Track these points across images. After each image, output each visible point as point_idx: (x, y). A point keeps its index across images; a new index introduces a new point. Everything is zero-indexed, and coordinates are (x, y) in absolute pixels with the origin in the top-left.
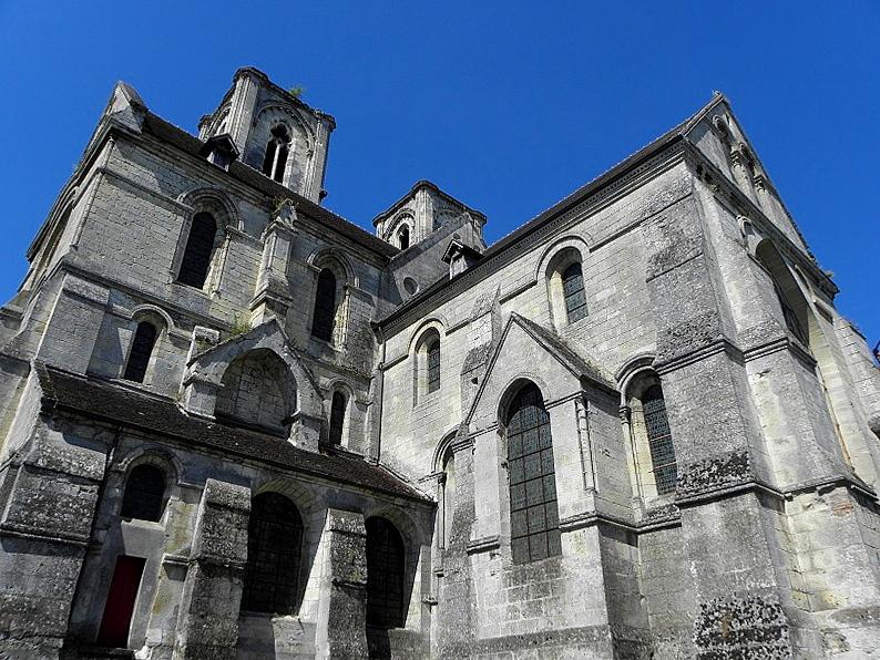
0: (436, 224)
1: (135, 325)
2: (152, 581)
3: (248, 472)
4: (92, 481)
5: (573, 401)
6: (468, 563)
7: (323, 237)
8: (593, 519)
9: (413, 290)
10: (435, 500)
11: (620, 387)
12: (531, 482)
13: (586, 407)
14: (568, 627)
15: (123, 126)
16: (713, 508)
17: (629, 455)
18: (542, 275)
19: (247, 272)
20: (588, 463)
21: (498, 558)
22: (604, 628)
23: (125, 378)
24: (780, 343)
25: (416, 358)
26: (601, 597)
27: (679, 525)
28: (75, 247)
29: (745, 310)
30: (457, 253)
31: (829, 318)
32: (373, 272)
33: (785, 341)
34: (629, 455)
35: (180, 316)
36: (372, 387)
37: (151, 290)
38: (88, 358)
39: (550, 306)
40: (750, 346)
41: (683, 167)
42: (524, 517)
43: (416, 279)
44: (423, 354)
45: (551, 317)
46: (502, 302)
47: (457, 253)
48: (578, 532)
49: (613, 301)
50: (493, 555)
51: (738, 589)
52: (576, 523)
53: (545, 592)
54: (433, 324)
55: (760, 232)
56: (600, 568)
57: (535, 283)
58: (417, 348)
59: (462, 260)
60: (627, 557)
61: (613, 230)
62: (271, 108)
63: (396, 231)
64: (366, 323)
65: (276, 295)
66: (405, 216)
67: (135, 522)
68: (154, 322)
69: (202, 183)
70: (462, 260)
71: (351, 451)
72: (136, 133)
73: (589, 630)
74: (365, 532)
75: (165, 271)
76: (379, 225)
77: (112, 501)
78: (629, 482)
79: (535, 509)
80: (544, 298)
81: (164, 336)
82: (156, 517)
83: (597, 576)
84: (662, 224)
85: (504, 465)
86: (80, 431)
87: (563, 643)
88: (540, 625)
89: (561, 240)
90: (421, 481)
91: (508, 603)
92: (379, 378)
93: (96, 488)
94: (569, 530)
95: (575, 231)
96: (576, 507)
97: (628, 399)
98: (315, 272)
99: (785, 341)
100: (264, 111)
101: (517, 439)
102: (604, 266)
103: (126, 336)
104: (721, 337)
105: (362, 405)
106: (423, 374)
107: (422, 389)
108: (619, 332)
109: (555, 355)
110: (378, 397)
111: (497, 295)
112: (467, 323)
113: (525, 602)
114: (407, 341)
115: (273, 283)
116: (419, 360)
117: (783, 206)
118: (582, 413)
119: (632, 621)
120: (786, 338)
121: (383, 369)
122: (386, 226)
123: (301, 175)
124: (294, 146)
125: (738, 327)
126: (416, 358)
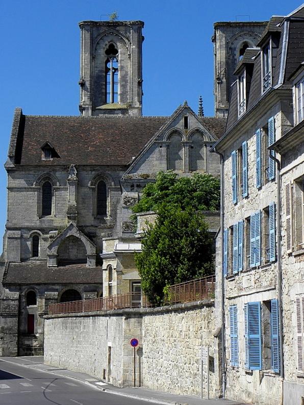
1: (31, 239)
3: (57, 287)
4: (16, 300)
7: (94, 170)
15: (9, 167)
23: (33, 256)
28: (8, 220)
35: (42, 230)
37: (33, 225)
38: (19, 256)
62: (101, 39)
65: (70, 214)
67: (30, 306)
69: (41, 173)
72: (13, 168)
75: (36, 216)
86: (12, 287)
98: (93, 189)
100: (98, 43)
103: (29, 243)
115: (70, 208)
123: (127, 74)
124: (120, 55)
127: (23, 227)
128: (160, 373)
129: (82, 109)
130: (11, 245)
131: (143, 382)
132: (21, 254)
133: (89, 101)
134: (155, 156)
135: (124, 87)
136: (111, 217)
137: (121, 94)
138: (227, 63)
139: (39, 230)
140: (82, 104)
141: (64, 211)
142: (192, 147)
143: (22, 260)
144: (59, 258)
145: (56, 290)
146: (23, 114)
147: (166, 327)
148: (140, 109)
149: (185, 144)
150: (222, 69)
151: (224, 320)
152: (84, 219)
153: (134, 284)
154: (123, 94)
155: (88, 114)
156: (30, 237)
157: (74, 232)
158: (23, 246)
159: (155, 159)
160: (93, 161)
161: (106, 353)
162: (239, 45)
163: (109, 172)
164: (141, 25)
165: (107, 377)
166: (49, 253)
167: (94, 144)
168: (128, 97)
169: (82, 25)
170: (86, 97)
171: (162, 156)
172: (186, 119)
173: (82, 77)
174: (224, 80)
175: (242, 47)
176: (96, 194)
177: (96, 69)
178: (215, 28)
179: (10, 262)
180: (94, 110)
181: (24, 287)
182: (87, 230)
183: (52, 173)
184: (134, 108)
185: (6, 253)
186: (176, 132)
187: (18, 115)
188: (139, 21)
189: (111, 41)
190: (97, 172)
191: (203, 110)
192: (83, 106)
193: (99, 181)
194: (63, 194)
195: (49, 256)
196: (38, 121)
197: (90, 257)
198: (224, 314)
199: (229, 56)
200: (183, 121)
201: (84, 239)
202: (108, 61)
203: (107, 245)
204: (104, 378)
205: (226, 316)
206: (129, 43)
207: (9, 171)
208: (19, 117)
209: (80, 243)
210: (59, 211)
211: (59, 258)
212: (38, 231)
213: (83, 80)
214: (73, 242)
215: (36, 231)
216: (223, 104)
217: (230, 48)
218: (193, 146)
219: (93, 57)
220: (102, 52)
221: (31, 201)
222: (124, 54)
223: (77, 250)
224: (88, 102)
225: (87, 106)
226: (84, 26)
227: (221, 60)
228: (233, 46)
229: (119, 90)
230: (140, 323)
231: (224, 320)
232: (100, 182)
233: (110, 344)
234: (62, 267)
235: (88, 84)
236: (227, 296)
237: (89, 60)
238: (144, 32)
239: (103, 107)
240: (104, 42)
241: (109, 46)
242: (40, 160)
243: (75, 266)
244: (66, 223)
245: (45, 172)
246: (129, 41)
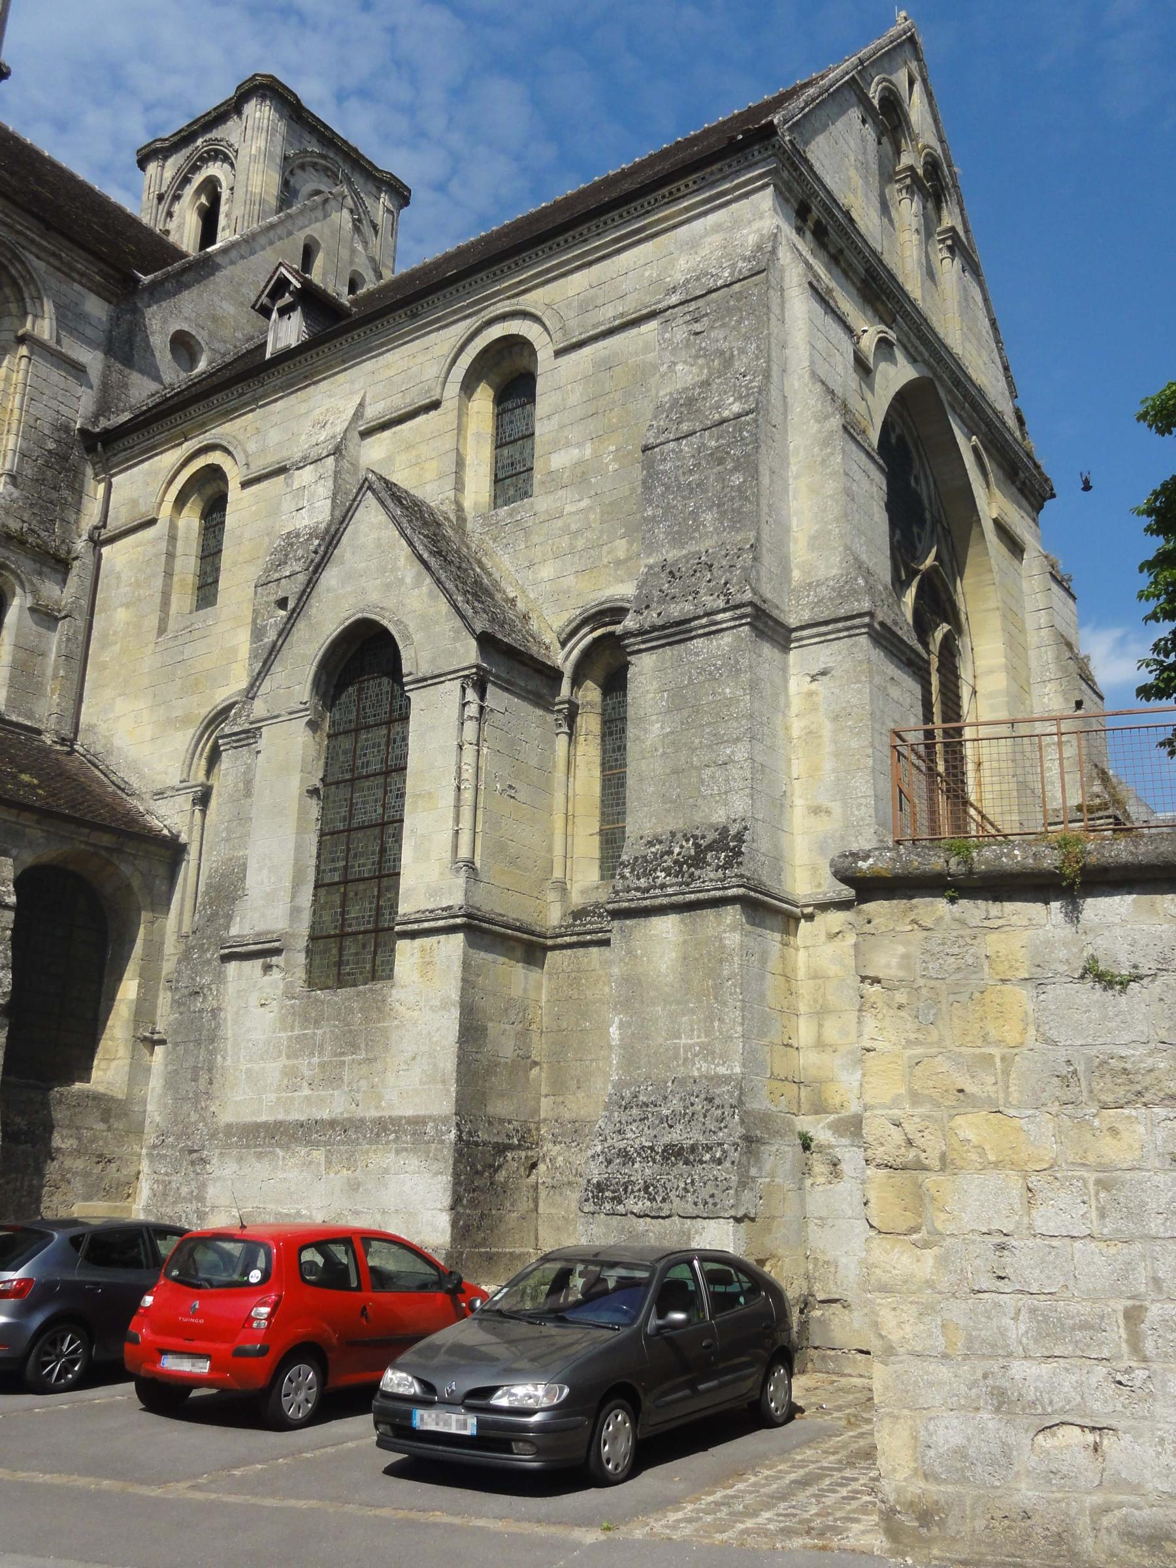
0: (288, 193)
5: (458, 683)
6: (220, 978)
8: (459, 921)
9: (193, 361)
10: (183, 838)
11: (564, 659)
12: (360, 834)
13: (482, 697)
14: (386, 1114)
16: (667, 927)
17: (559, 797)
18: (453, 389)
20: (466, 812)
21: (276, 975)
22: (445, 1120)
24: (857, 621)
25: (173, 527)
26: (449, 1064)
27: (606, 943)
29: (816, 542)
30: (287, 298)
31: (1016, 548)
32: (96, 308)
33: (867, 620)
34: (559, 797)
36: (73, 580)
39: (460, 463)
40: (806, 616)
41: (766, 199)
42: (337, 898)
43: (201, 336)
44: (191, 520)
45: (459, 486)
46: (365, 434)
47: (287, 298)
48: (432, 940)
49: (581, 476)
50: (267, 968)
51: (681, 1072)
52: (426, 925)
53: (354, 1047)
54: (215, 458)
55: (913, 360)
56: (455, 1013)
57: (435, 405)
58: (181, 501)
59: (297, 317)
60: (516, 992)
61: (608, 315)
63: (189, 190)
64: (66, 429)
66: (217, 155)
70: (297, 317)
71: (14, 718)
73: (418, 1122)
74: (12, 900)
76: (152, 167)
78: (550, 849)
79: (361, 886)
80: (449, 442)
83: (449, 1025)
84: (697, 327)
85: (314, 792)
87: (370, 1142)
88: (335, 1105)
89: (503, 317)
90: (160, 794)
91: (283, 1061)
92: (89, 560)
94: (413, 935)
95: (533, 300)
96: (433, 893)
97: (576, 682)
99: (867, 620)
101: (346, 743)
102: (575, 396)
104: (748, 596)
105: (46, 616)
106: (188, 564)
107: (183, 598)
108: (580, 543)
109: (438, 582)
110: (84, 603)
111: (358, 414)
112: (282, 470)
113: (316, 1060)
114: (158, 486)
116: (181, 533)
117: (986, 300)
118: (472, 710)
119: (498, 1107)
120: (870, 614)
121: (97, 542)
122: (169, 174)
125: (796, 574)
126: (173, 527)
136: (15, 485)
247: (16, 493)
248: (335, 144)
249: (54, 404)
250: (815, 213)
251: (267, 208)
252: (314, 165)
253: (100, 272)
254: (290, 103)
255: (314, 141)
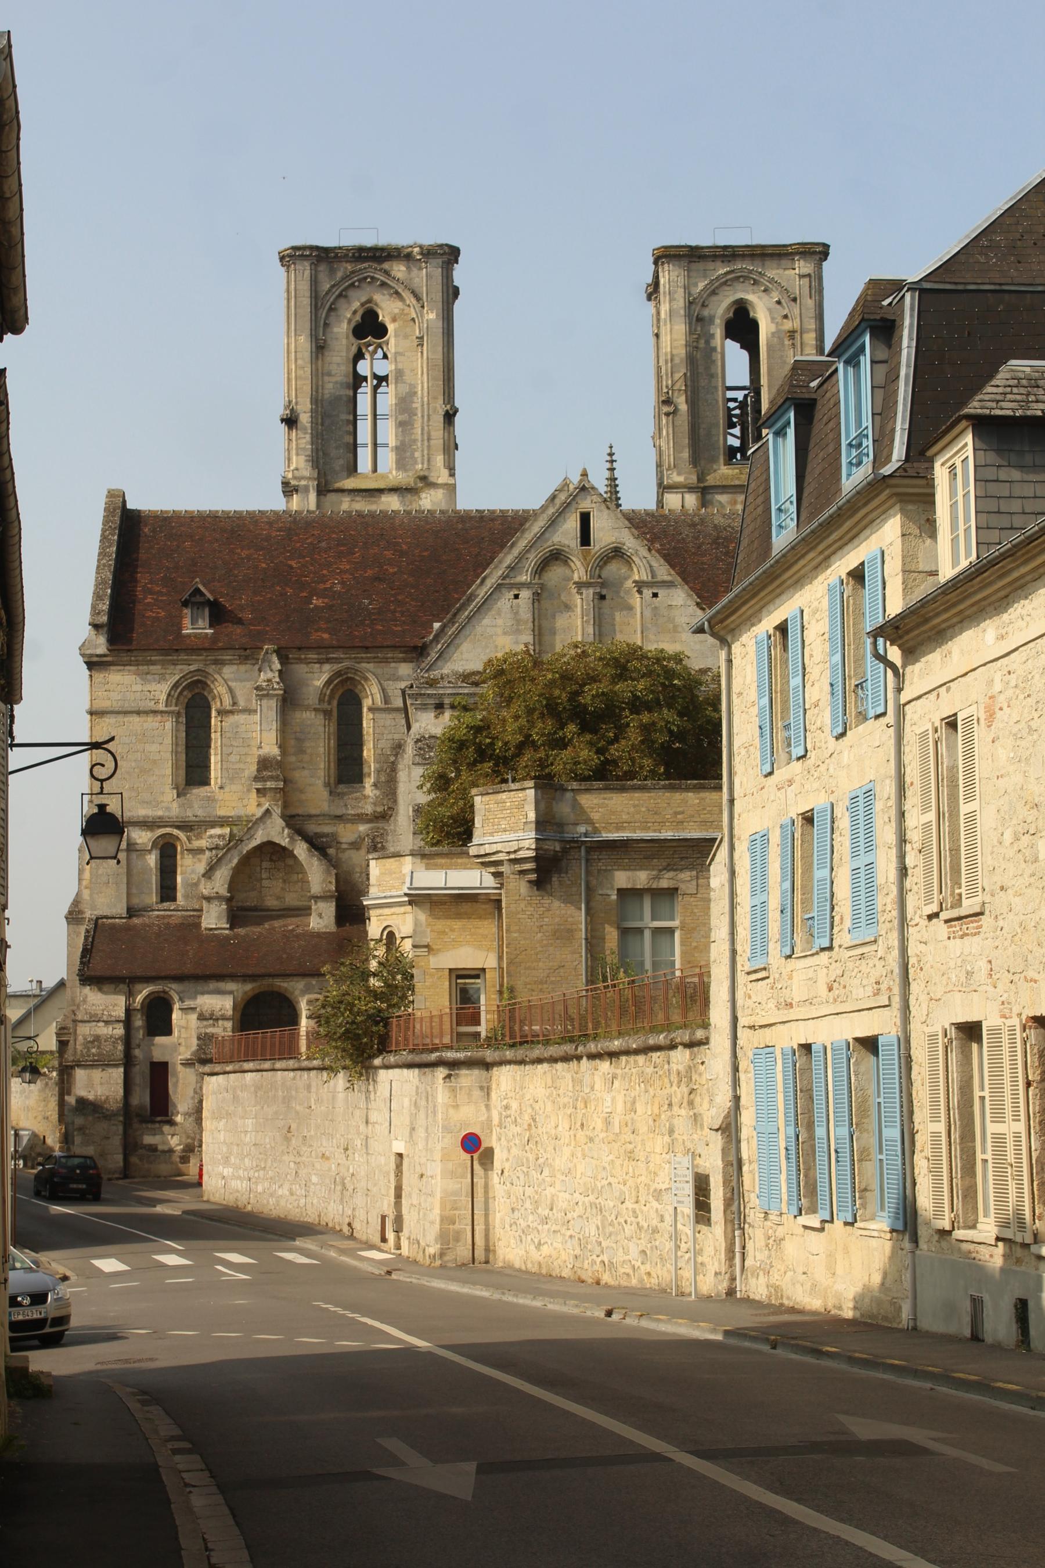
2: (175, 1074)
3: (231, 986)
7: (328, 661)
15: (91, 656)
19: (244, 751)
37: (160, 813)
38: (125, 900)
62: (340, 295)
68: (171, 841)
72: (105, 656)
77: (138, 1029)
81: (182, 853)
82: (168, 1031)
86: (106, 988)
93: (121, 1025)
100: (331, 309)
115: (264, 763)
124: (392, 342)
127: (135, 820)
128: (546, 1227)
129: (289, 489)
130: (100, 872)
131: (494, 1251)
132: (129, 895)
133: (309, 469)
134: (500, 622)
135: (404, 426)
137: (397, 448)
138: (691, 360)
139: (178, 827)
140: (290, 476)
141: (247, 773)
142: (603, 597)
143: (132, 912)
144: (234, 904)
145: (231, 992)
146: (129, 506)
147: (566, 1100)
148: (451, 489)
149: (580, 585)
150: (677, 376)
151: (736, 1083)
152: (303, 797)
153: (459, 981)
154: (403, 452)
155: (306, 503)
156: (155, 844)
157: (276, 831)
158: (135, 871)
159: (499, 631)
160: (326, 636)
161: (388, 1173)
162: (721, 309)
163: (371, 665)
164: (450, 255)
165: (391, 1236)
166: (205, 892)
167: (326, 589)
168: (417, 454)
169: (289, 256)
170: (302, 458)
171: (518, 622)
172: (585, 519)
173: (290, 402)
174: (683, 407)
175: (731, 315)
176: (333, 728)
177: (326, 378)
178: (656, 263)
179: (97, 919)
180: (323, 490)
181: (138, 986)
182: (312, 828)
183: (211, 669)
184: (433, 485)
185: (86, 894)
186: (557, 557)
187: (114, 510)
188: (447, 245)
189: (370, 301)
190: (336, 667)
191: (617, 486)
192: (293, 482)
193: (340, 692)
194: (243, 728)
195: (208, 899)
196: (166, 521)
197: (316, 898)
198: (736, 1069)
199: (697, 340)
200: (572, 524)
201: (301, 850)
202: (359, 356)
203: (381, 874)
204: (384, 1240)
205: (742, 1076)
206: (418, 306)
207: (93, 664)
208: (117, 519)
209: (290, 862)
210: (231, 775)
211: (234, 904)
212: (176, 832)
213: (292, 410)
214: (271, 860)
215: (168, 830)
216: (679, 474)
217: (700, 319)
218: (604, 592)
219: (320, 347)
220: (342, 329)
221: (154, 748)
222: (406, 337)
223: (284, 881)
224: (306, 470)
225: (303, 483)
226: (291, 257)
227: (675, 352)
228: (706, 313)
229: (388, 433)
230: (486, 1090)
231: (736, 1083)
232: (342, 695)
233: (399, 1147)
234: (241, 931)
235: (305, 419)
236: (742, 1021)
237: (307, 355)
238: (460, 275)
239: (349, 483)
240: (349, 303)
241: (363, 317)
242: (179, 635)
243: (277, 924)
244: (252, 806)
245: (192, 668)
246: (418, 298)
247: (378, 793)
248: (739, 255)
249: (390, 737)
250: (447, 701)
251: (677, 360)
252: (725, 283)
253: (401, 652)
254: (684, 256)
255: (719, 263)
